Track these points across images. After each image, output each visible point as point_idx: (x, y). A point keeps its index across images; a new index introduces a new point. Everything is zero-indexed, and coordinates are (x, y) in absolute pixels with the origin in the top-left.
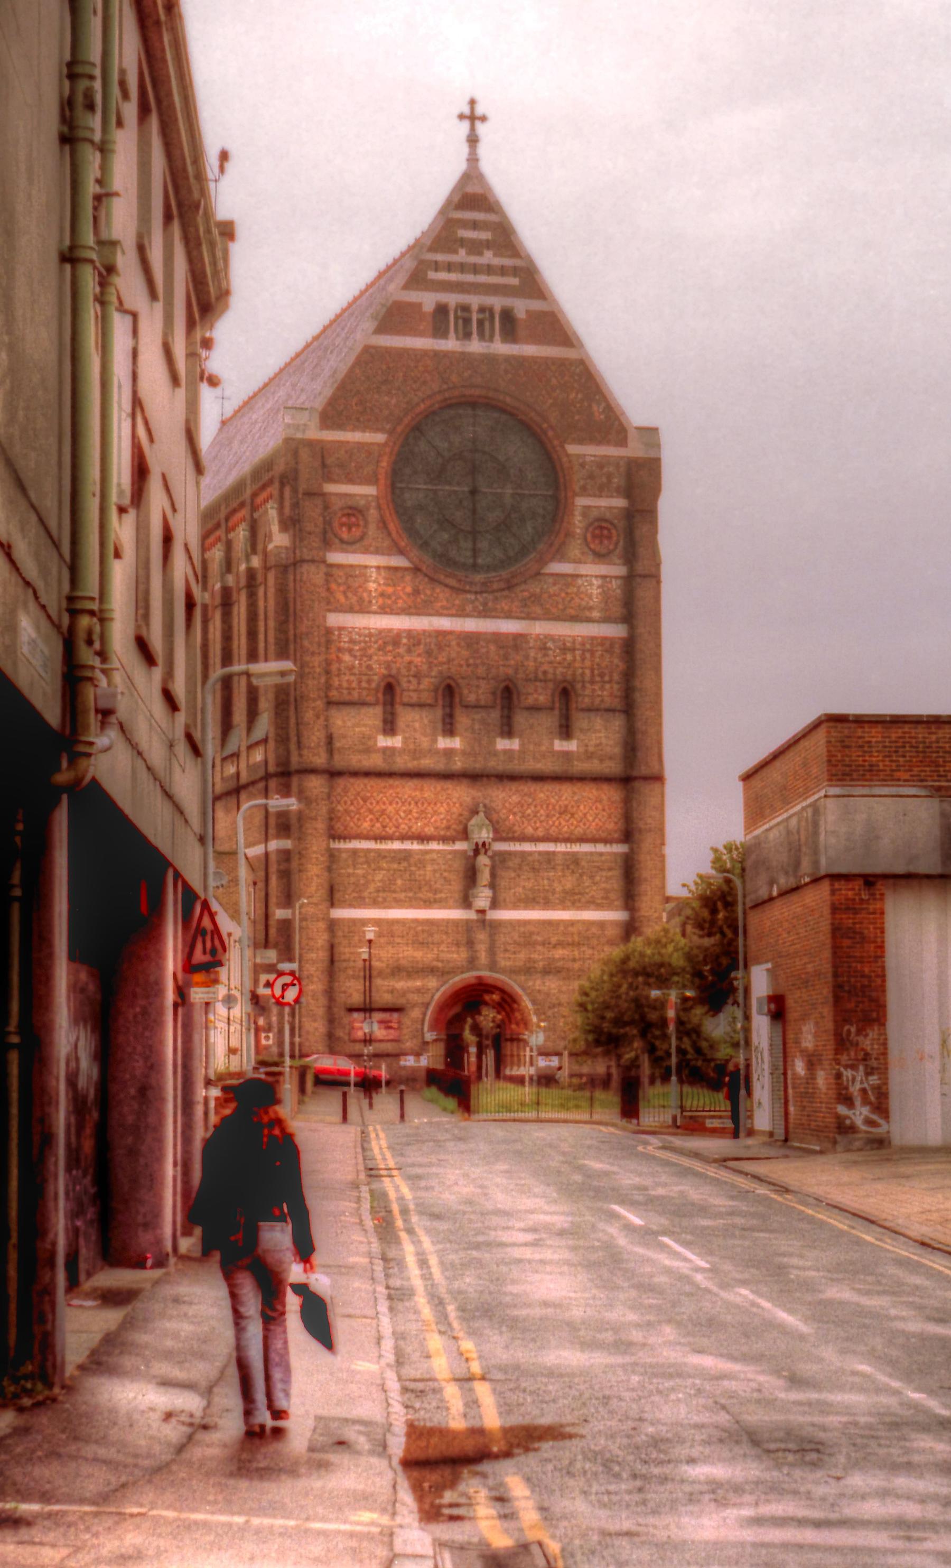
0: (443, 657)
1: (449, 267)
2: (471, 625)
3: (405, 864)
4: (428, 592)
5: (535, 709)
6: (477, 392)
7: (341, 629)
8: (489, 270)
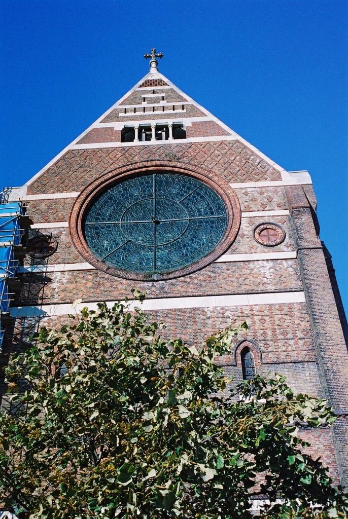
4: (108, 285)
6: (154, 163)
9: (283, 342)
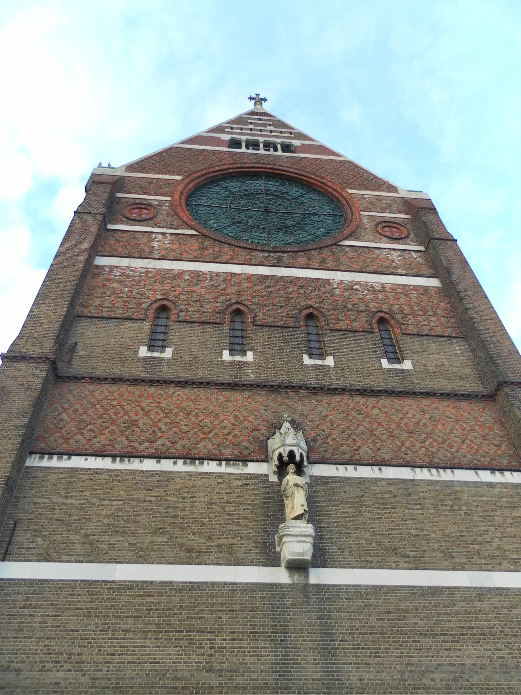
3: (160, 492)
7: (112, 267)
9: (424, 317)
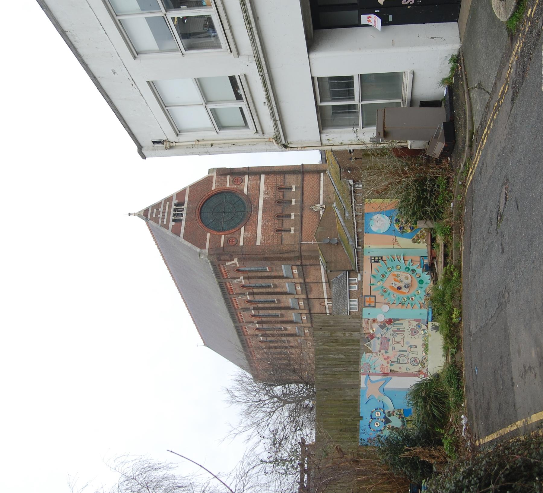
0: (269, 218)
1: (163, 219)
2: (260, 212)
5: (284, 196)
6: (197, 211)
8: (164, 209)
